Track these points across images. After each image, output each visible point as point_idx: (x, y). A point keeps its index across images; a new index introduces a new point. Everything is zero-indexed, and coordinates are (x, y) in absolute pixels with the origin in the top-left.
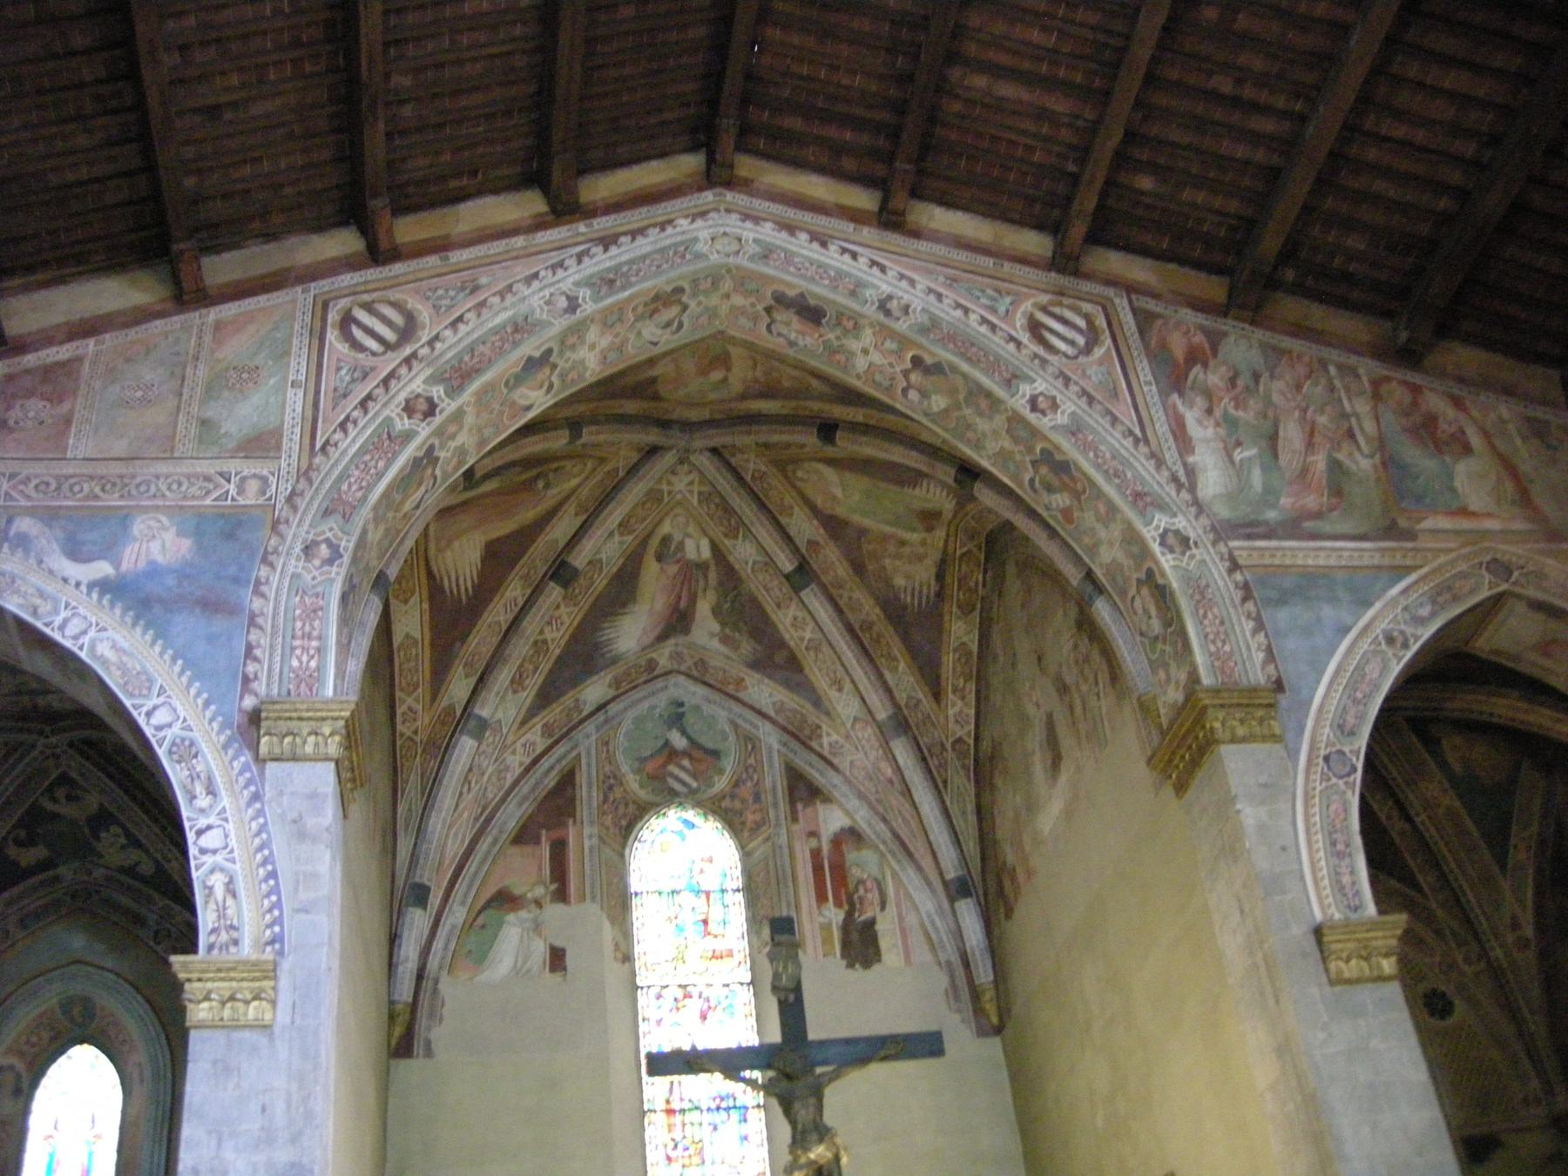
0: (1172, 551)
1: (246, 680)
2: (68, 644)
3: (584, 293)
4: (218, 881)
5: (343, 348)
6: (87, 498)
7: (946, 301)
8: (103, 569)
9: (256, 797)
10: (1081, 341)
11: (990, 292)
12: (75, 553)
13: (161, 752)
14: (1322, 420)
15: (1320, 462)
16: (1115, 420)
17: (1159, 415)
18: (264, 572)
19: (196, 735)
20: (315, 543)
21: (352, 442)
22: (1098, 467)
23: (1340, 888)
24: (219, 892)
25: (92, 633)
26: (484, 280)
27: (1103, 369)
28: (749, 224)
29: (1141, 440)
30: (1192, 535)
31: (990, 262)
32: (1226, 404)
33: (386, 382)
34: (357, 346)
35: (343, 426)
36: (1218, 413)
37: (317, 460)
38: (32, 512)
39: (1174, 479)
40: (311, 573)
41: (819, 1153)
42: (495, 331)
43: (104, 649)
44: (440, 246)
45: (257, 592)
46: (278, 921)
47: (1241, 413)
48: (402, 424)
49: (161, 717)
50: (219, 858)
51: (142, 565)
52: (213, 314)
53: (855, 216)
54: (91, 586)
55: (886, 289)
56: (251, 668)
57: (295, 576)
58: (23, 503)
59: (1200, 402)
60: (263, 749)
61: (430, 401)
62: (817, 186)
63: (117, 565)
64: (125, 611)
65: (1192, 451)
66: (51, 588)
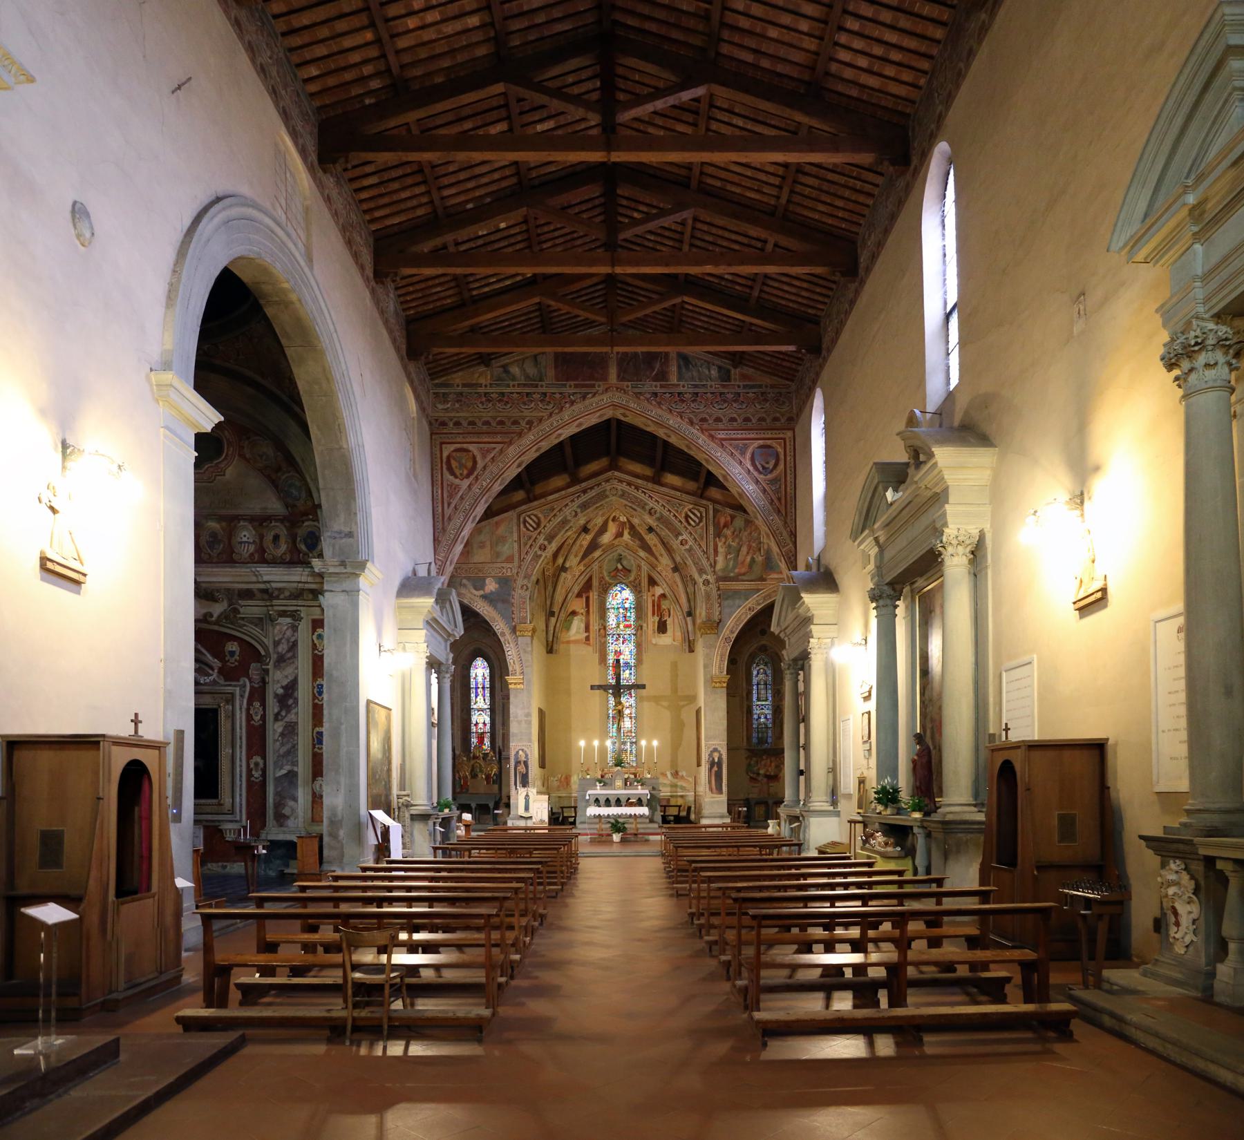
3: (579, 510)
8: (481, 592)
12: (476, 589)
15: (749, 559)
16: (700, 547)
17: (712, 544)
21: (529, 557)
23: (720, 668)
31: (678, 494)
32: (730, 540)
33: (534, 541)
34: (528, 529)
41: (620, 707)
44: (544, 495)
48: (539, 553)
52: (496, 519)
59: (723, 540)
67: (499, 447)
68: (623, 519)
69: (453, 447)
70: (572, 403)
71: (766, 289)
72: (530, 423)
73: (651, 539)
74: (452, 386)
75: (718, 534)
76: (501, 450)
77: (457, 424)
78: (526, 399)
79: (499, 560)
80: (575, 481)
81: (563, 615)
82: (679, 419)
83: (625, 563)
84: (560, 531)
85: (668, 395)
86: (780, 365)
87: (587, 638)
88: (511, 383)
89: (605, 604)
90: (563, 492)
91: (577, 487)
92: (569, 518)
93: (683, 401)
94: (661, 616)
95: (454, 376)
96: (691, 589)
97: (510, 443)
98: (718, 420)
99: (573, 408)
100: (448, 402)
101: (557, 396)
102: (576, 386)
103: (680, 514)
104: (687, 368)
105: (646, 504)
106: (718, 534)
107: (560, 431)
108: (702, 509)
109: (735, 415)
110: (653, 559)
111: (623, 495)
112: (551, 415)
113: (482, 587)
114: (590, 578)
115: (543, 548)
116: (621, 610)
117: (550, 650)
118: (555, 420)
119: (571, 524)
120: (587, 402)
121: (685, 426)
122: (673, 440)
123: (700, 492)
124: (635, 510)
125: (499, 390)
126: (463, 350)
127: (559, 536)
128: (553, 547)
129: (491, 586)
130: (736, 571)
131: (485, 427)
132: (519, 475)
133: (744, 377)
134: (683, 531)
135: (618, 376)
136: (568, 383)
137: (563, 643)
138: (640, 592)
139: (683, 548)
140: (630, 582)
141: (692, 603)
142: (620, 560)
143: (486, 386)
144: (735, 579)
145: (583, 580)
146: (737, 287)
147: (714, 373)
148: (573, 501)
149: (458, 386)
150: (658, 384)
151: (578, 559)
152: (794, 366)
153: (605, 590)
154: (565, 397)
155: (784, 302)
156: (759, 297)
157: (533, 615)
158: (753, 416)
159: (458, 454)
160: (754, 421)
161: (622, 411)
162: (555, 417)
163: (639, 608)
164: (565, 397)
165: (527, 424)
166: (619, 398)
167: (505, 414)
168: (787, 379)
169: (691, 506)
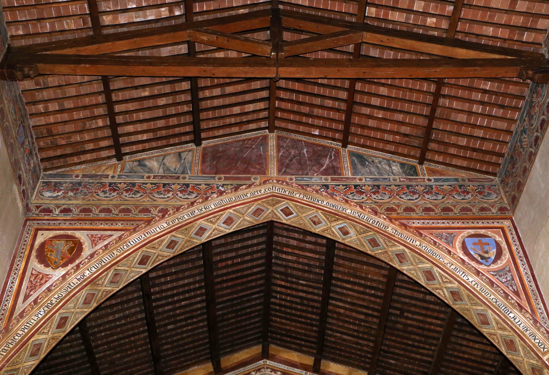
67: (117, 234)
69: (51, 234)
70: (221, 193)
72: (164, 212)
76: (120, 238)
82: (358, 208)
88: (147, 175)
93: (361, 193)
95: (73, 168)
97: (135, 231)
99: (221, 198)
100: (59, 191)
101: (203, 187)
102: (226, 179)
104: (363, 164)
109: (430, 206)
112: (192, 204)
118: (197, 210)
120: (240, 192)
125: (129, 180)
131: (103, 215)
133: (432, 172)
135: (279, 171)
136: (217, 176)
147: (396, 168)
149: (77, 176)
150: (329, 177)
158: (455, 206)
160: (455, 211)
168: (487, 173)
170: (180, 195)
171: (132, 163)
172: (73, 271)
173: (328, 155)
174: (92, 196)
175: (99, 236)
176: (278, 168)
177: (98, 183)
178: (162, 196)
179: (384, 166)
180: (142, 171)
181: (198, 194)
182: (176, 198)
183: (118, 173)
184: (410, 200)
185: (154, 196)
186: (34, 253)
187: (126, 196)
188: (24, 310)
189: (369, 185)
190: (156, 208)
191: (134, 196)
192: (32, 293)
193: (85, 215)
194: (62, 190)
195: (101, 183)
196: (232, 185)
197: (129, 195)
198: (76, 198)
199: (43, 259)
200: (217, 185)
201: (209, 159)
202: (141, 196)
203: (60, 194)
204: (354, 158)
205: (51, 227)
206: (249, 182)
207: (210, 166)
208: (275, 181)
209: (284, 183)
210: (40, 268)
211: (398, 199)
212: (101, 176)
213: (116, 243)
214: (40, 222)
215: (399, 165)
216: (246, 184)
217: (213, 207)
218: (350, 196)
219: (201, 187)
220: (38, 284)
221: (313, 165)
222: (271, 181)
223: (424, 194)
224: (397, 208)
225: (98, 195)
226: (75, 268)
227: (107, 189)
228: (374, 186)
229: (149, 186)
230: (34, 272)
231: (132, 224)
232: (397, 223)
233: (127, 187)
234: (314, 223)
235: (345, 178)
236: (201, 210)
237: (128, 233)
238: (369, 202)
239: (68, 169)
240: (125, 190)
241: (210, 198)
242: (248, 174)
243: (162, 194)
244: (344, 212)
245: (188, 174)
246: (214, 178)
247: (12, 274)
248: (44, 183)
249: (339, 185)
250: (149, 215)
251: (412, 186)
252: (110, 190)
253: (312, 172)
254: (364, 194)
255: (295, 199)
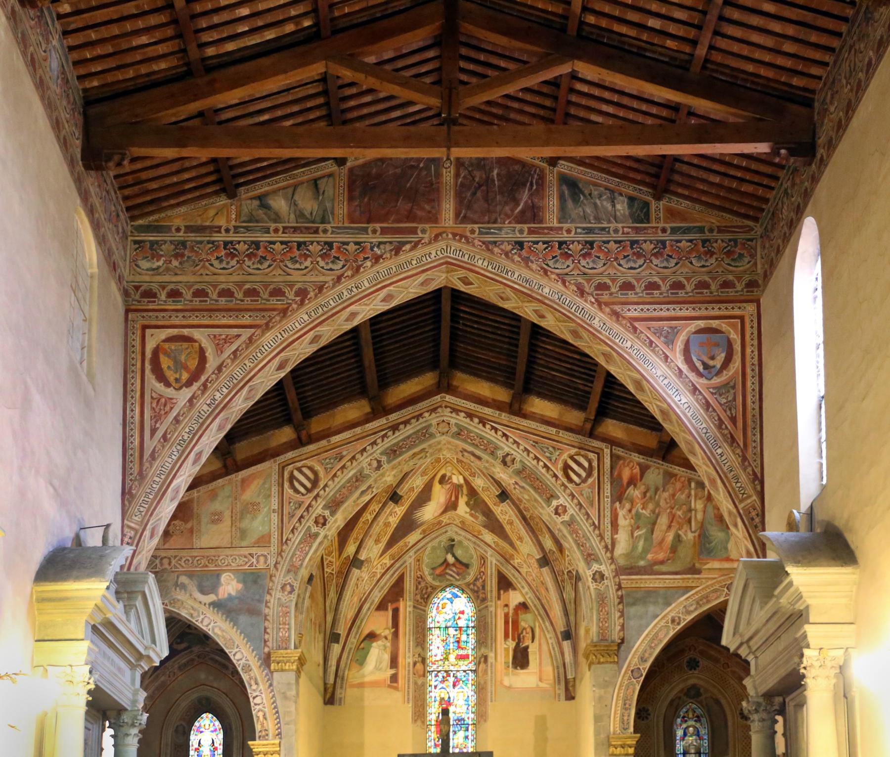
0: (596, 582)
1: (265, 642)
2: (204, 628)
3: (384, 459)
4: (261, 714)
5: (291, 491)
6: (203, 567)
7: (531, 455)
8: (212, 598)
9: (271, 685)
10: (584, 474)
11: (551, 449)
12: (203, 592)
13: (239, 669)
14: (679, 513)
17: (608, 513)
18: (268, 597)
19: (250, 663)
20: (285, 585)
21: (298, 537)
22: (576, 541)
24: (261, 718)
25: (212, 624)
26: (344, 453)
27: (590, 490)
28: (454, 415)
29: (596, 527)
30: (606, 574)
31: (553, 430)
33: (307, 509)
34: (296, 491)
35: (292, 531)
36: (634, 511)
37: (284, 547)
38: (186, 573)
39: (606, 547)
40: (284, 597)
42: (348, 481)
43: (217, 630)
44: (327, 434)
45: (267, 607)
46: (280, 728)
47: (644, 511)
48: (314, 529)
49: (238, 656)
50: (260, 707)
51: (226, 596)
53: (498, 406)
54: (210, 604)
55: (507, 449)
56: (267, 637)
57: (279, 599)
58: (182, 569)
59: (628, 506)
60: (272, 668)
61: (324, 517)
62: (484, 389)
63: (217, 595)
64: (223, 614)
65: (617, 533)
66: (196, 605)
67: (246, 333)
68: (457, 479)
70: (377, 259)
71: (722, 43)
72: (302, 293)
73: (504, 512)
74: (168, 229)
75: (619, 496)
76: (250, 339)
77: (174, 294)
78: (297, 253)
79: (244, 544)
80: (379, 410)
81: (353, 641)
82: (560, 286)
83: (459, 552)
84: (351, 493)
85: (541, 246)
86: (737, 191)
87: (394, 678)
88: (273, 226)
89: (424, 621)
90: (358, 430)
91: (382, 421)
92: (366, 472)
93: (567, 256)
94: (519, 639)
96: (569, 593)
97: (267, 327)
98: (627, 286)
99: (377, 268)
100: (159, 257)
101: (352, 247)
102: (384, 231)
103: (555, 463)
104: (576, 201)
105: (497, 448)
106: (619, 496)
107: (353, 308)
108: (591, 455)
109: (656, 279)
110: (507, 547)
111: (459, 433)
112: (339, 278)
113: (214, 589)
114: (401, 580)
115: (322, 522)
116: (452, 631)
117: (330, 698)
119: (370, 481)
120: (403, 258)
121: (570, 296)
122: (549, 323)
123: (588, 426)
124: (479, 458)
126: (185, 152)
127: (349, 503)
128: (339, 520)
129: (230, 586)
130: (650, 556)
131: (223, 301)
132: (279, 386)
133: (672, 214)
134: (559, 491)
135: (457, 215)
137: (354, 686)
138: (484, 600)
139: (559, 520)
140: (468, 585)
141: (572, 618)
142: (450, 548)
143: (227, 231)
144: (648, 570)
145: (389, 580)
146: (669, 43)
147: (622, 207)
148: (374, 443)
149: (178, 230)
150: (525, 227)
151: (382, 546)
152: (760, 192)
153: (425, 596)
154: (363, 250)
155: (750, 68)
156: (706, 60)
157: (300, 635)
159: (173, 346)
161: (462, 273)
162: (346, 284)
163: (482, 627)
164: (363, 250)
165: (297, 294)
166: (455, 250)
167: (258, 278)
169: (573, 451)
170: (322, 263)
171: (249, 202)
172: (199, 392)
173: (527, 181)
174: (204, 267)
175: (223, 337)
176: (456, 208)
177: (209, 242)
178: (297, 266)
179: (605, 203)
180: (266, 218)
181: (346, 261)
182: (317, 269)
183: (233, 223)
184: (631, 268)
185: (286, 266)
186: (148, 367)
187: (249, 267)
188: (154, 450)
189: (579, 242)
190: (291, 287)
191: (259, 266)
192: (158, 425)
193: (201, 301)
194: (162, 256)
195: (213, 242)
196: (391, 243)
197: (253, 264)
198: (184, 273)
199: (161, 377)
200: (371, 243)
201: (357, 193)
202: (270, 266)
203: (160, 263)
204: (564, 188)
205: (160, 323)
206: (414, 238)
207: (360, 207)
208: (450, 236)
209: (463, 240)
210: (160, 387)
211: (615, 268)
212: (211, 228)
213: (247, 348)
214: (145, 314)
215: (626, 200)
216: (410, 242)
217: (367, 285)
218: (551, 263)
219: (348, 247)
220: (163, 412)
221: (506, 203)
222: (444, 235)
223: (653, 258)
224: (611, 284)
225: (212, 265)
226: (202, 388)
227: (223, 253)
228: (586, 242)
229: (278, 246)
230: (154, 395)
231: (264, 316)
232: (607, 310)
233: (248, 250)
234: (502, 298)
235: (547, 228)
236: (351, 291)
237: (259, 331)
238: (575, 272)
239: (163, 215)
240: (247, 256)
241: (362, 269)
242: (413, 222)
243: (297, 262)
244: (540, 291)
245: (329, 223)
246: (365, 230)
247: (129, 397)
248: (135, 242)
249: (537, 243)
250: (283, 300)
251: (637, 242)
252: (227, 255)
253: (502, 216)
254: (571, 258)
255: (477, 269)
